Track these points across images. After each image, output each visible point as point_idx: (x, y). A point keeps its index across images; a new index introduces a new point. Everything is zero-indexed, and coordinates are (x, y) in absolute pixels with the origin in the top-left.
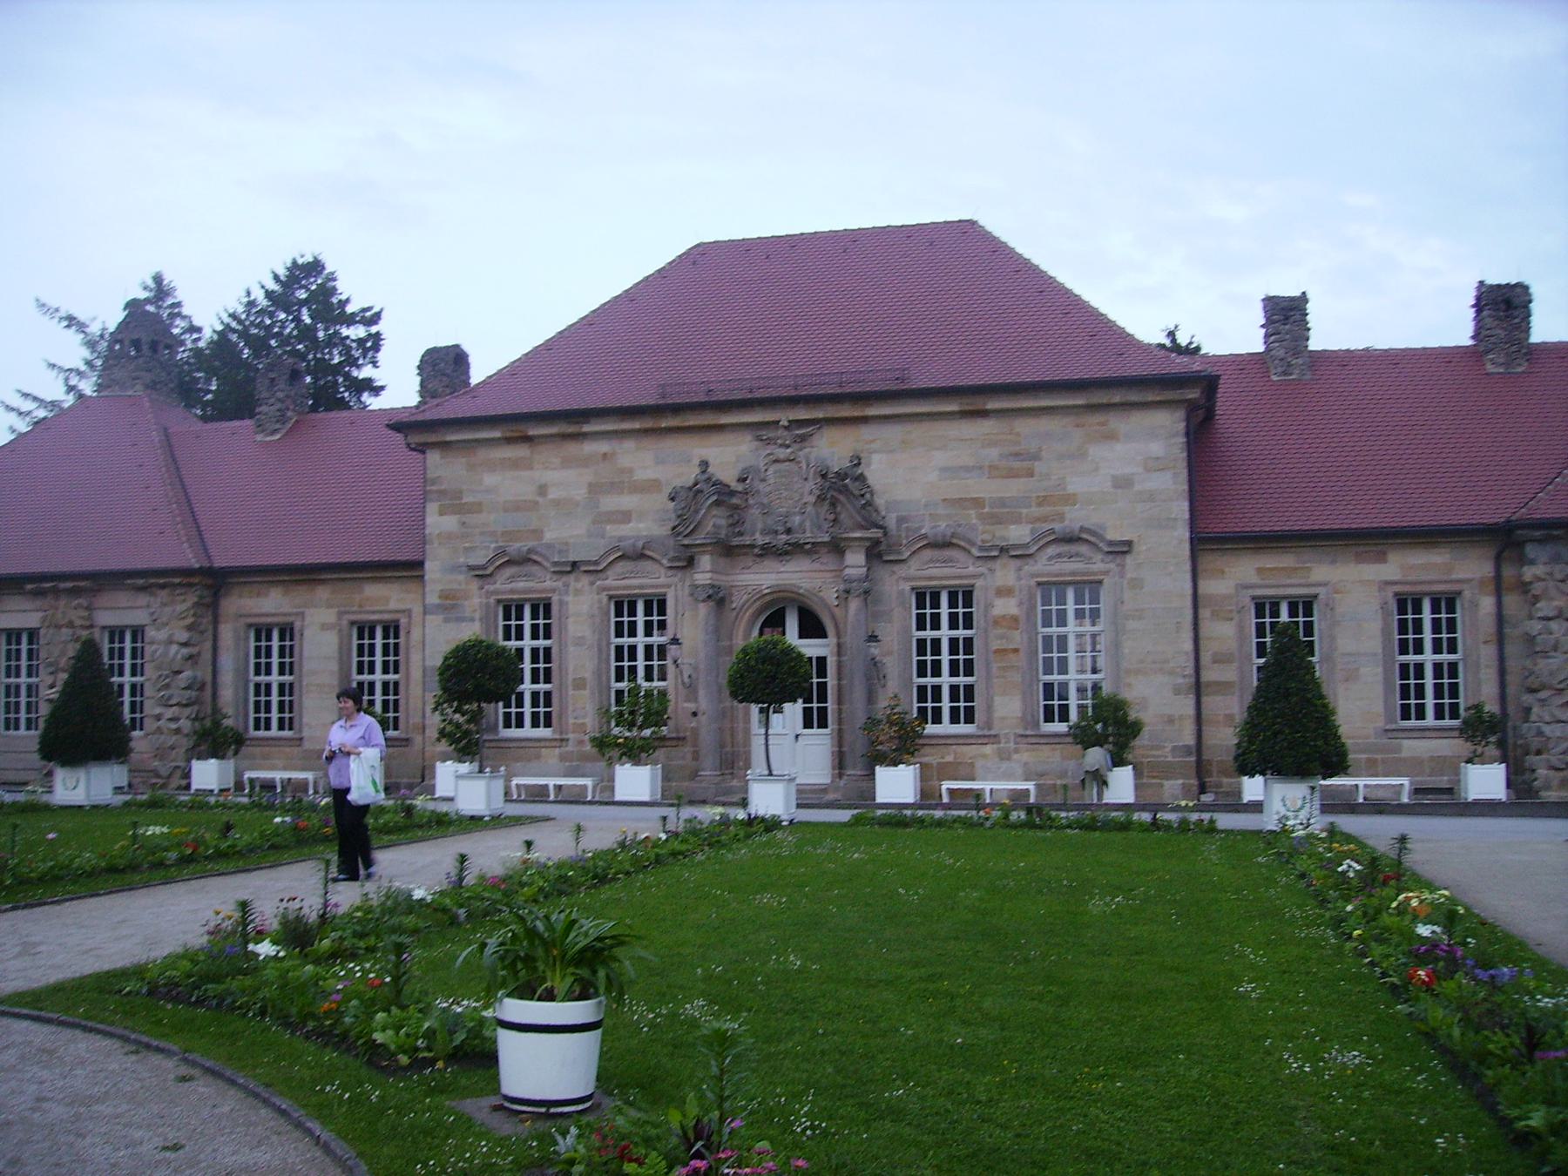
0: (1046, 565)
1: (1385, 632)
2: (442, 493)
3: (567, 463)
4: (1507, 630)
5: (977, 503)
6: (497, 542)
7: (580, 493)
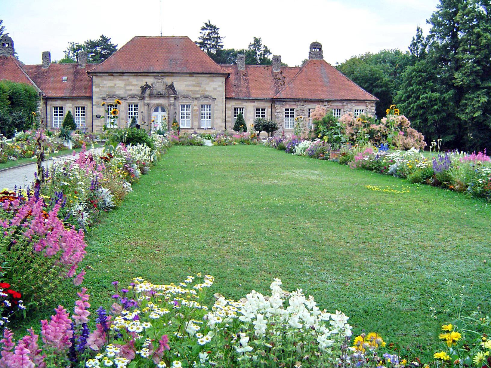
0: (203, 101)
1: (254, 114)
3: (120, 80)
5: (192, 91)
7: (123, 86)
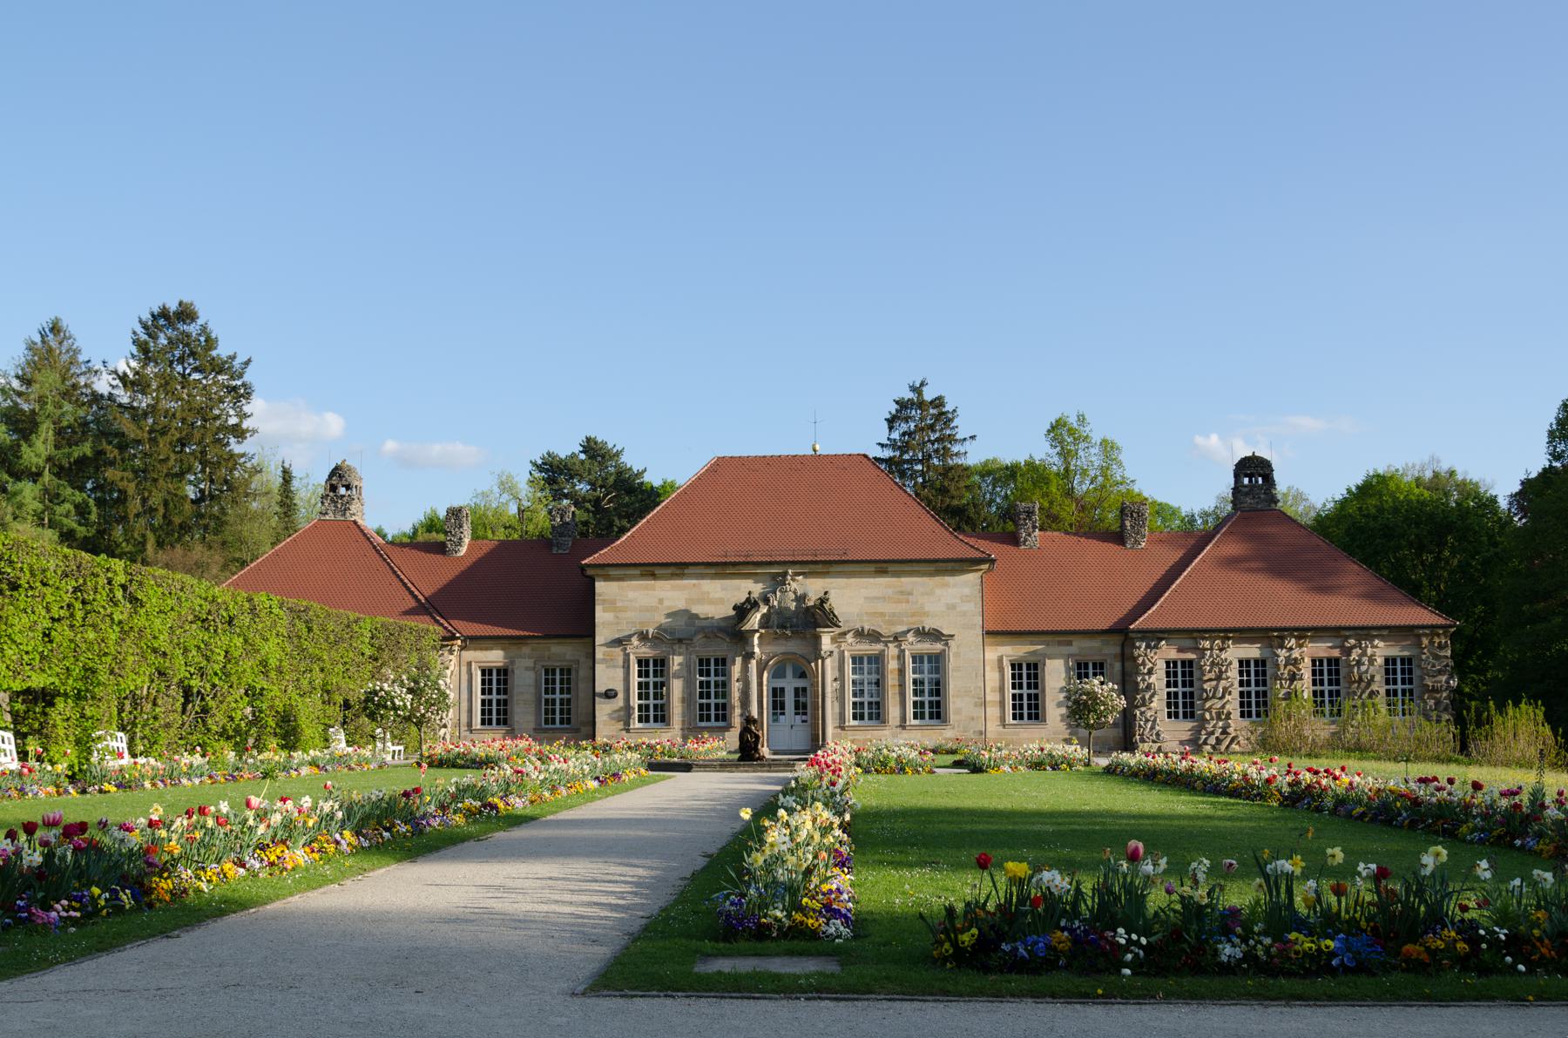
2: (604, 600)
4: (1127, 678)
5: (882, 614)
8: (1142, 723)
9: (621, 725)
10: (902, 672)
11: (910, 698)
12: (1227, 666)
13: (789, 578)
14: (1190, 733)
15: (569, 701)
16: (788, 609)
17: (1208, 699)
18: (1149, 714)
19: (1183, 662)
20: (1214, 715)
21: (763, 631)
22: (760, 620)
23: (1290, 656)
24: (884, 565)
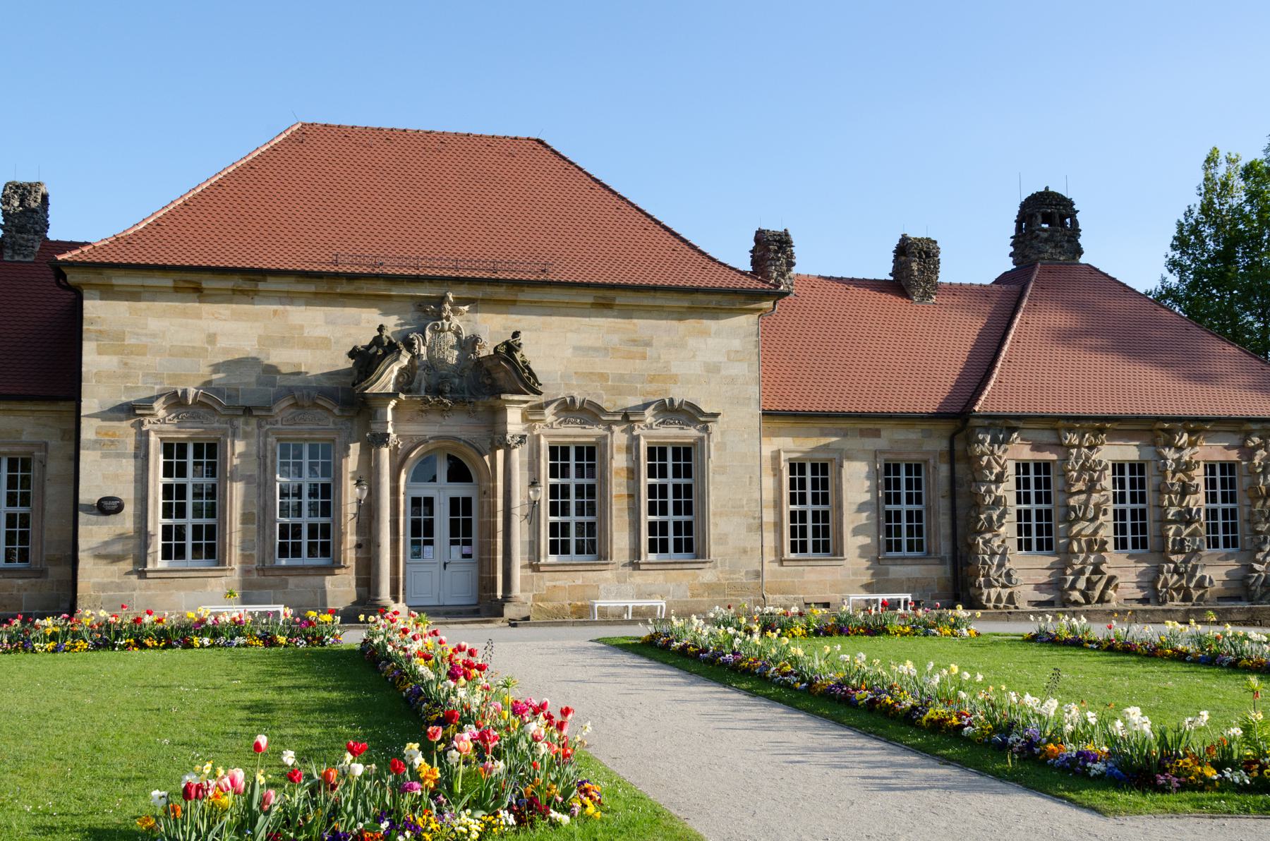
5: (603, 377)
6: (161, 383)
8: (986, 557)
9: (127, 565)
10: (633, 473)
11: (646, 518)
12: (1101, 471)
13: (448, 306)
14: (1049, 572)
15: (25, 518)
16: (443, 361)
17: (1077, 519)
18: (996, 542)
19: (1037, 465)
20: (1083, 544)
21: (402, 396)
22: (397, 378)
23: (1180, 458)
24: (609, 294)
